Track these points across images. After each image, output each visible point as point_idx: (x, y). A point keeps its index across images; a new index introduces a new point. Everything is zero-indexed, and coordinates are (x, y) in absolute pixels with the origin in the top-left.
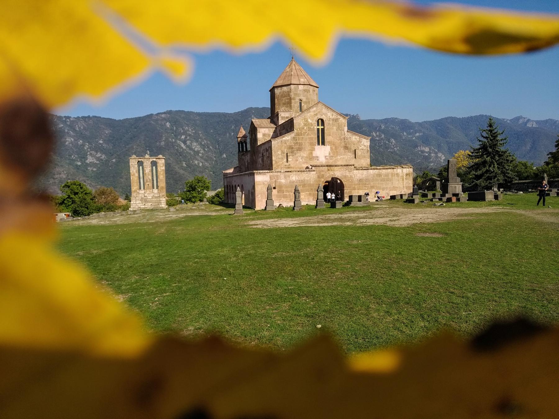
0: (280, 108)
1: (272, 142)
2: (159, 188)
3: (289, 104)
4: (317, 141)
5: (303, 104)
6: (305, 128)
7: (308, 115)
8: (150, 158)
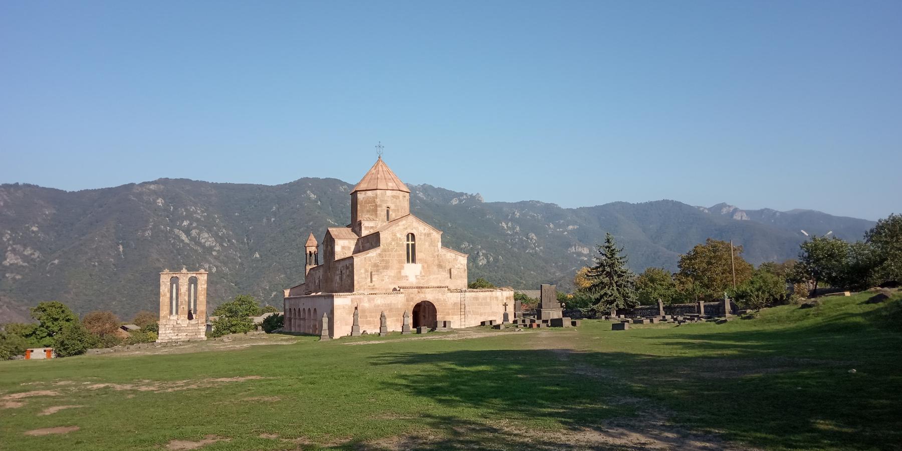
0: (363, 216)
1: (355, 259)
2: (198, 313)
3: (374, 211)
4: (406, 258)
5: (391, 213)
6: (393, 243)
7: (397, 228)
8: (188, 272)
